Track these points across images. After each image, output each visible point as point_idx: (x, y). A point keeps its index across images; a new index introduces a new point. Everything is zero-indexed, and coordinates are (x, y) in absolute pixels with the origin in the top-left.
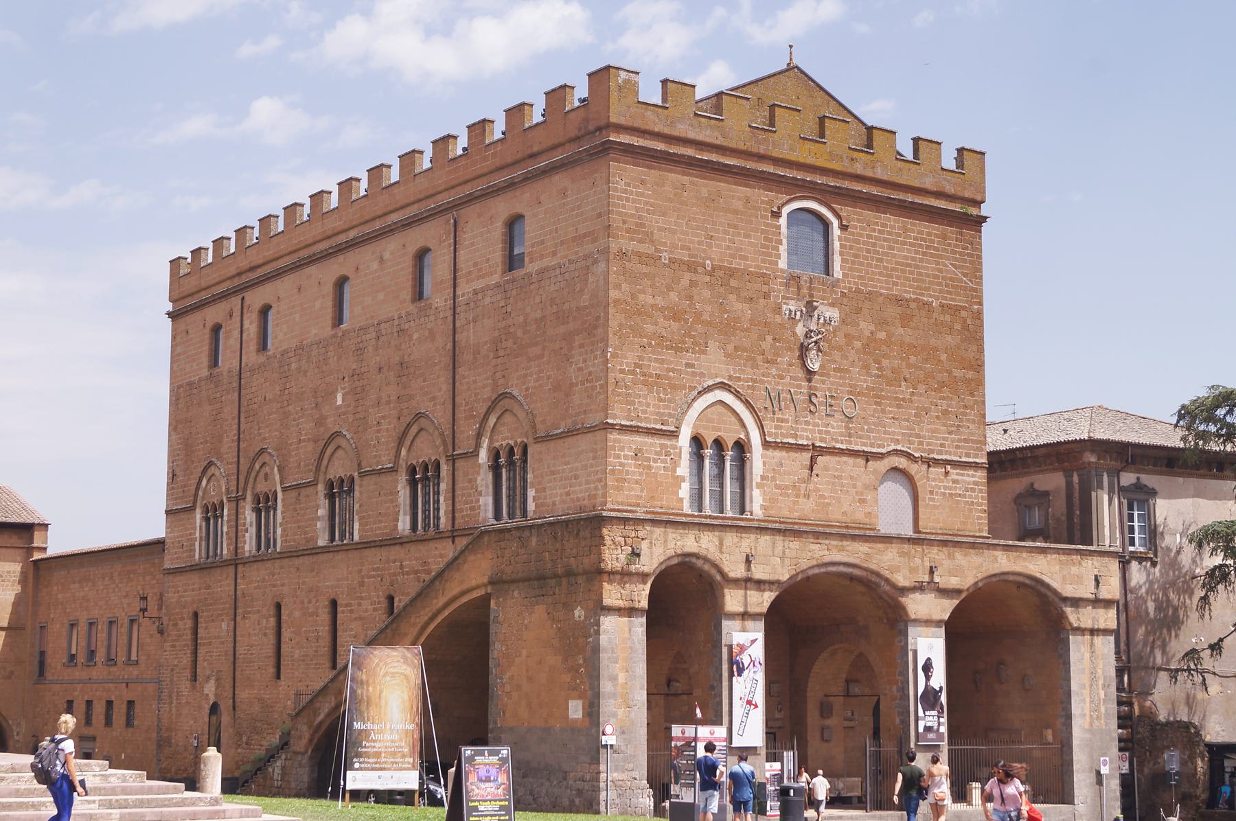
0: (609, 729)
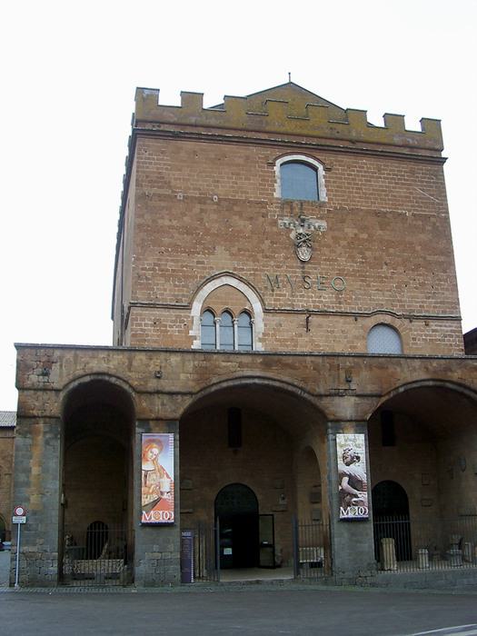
0: (20, 511)
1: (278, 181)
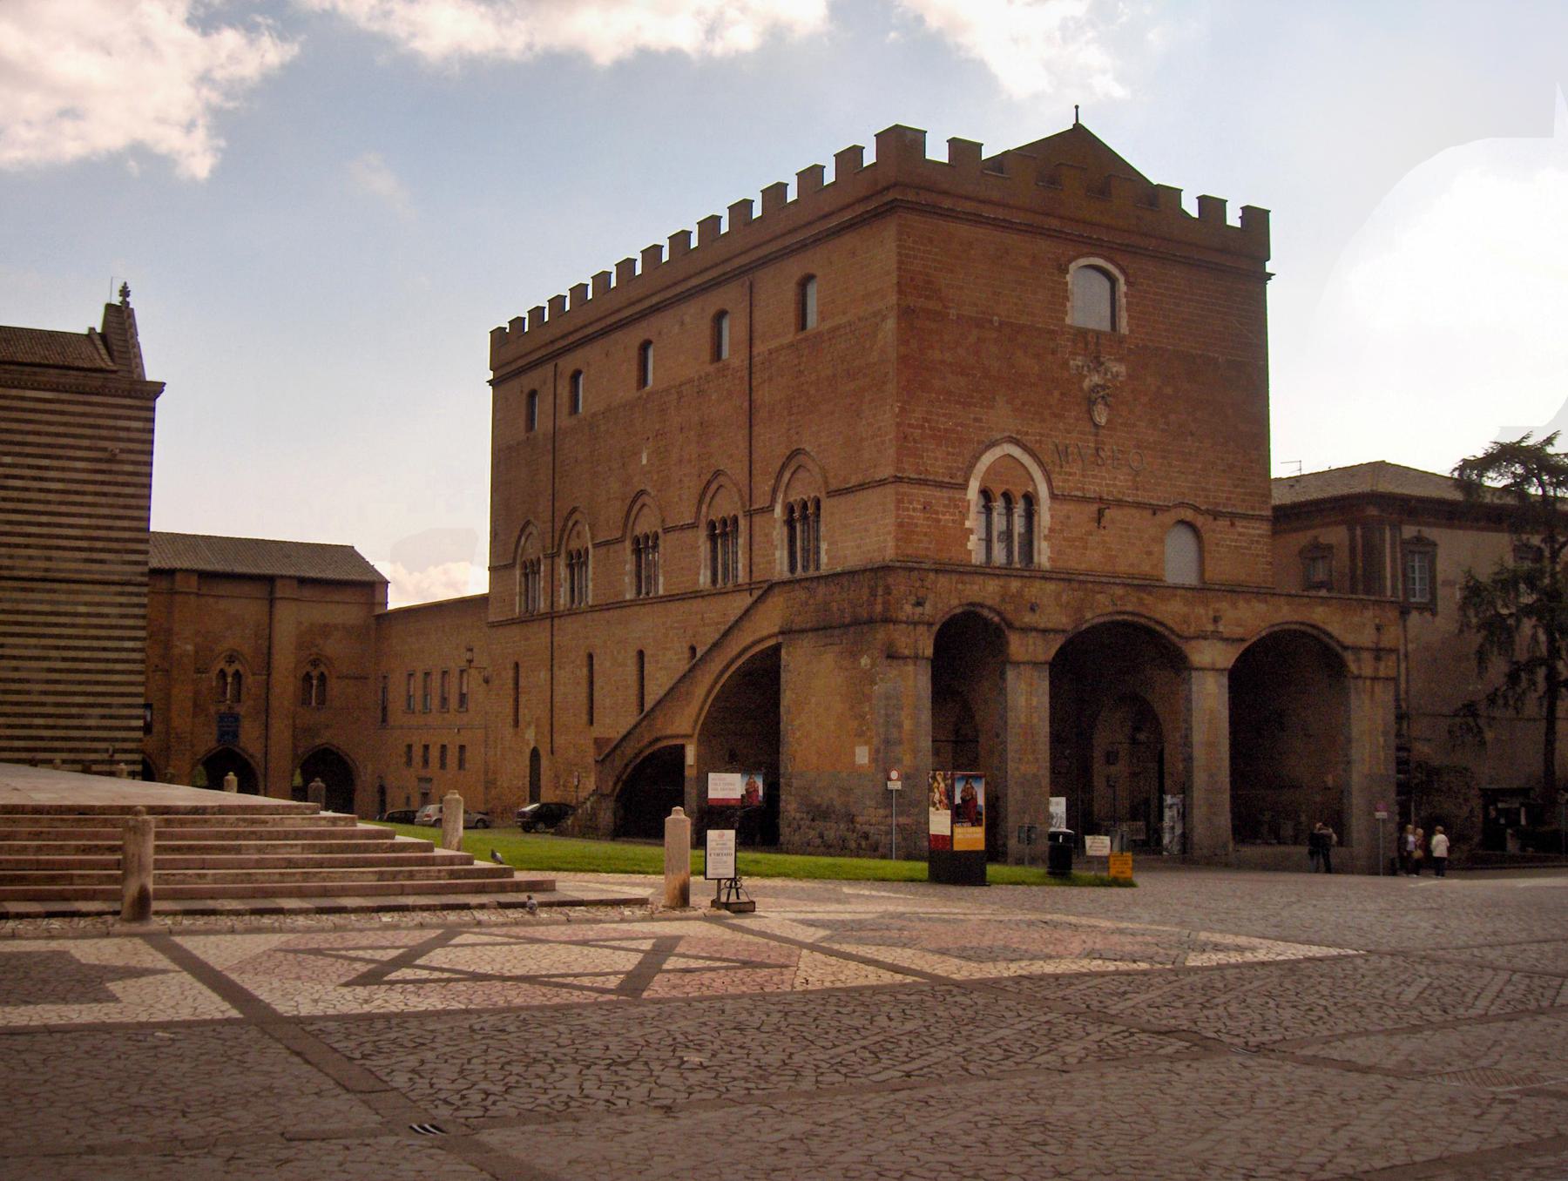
0: (894, 775)
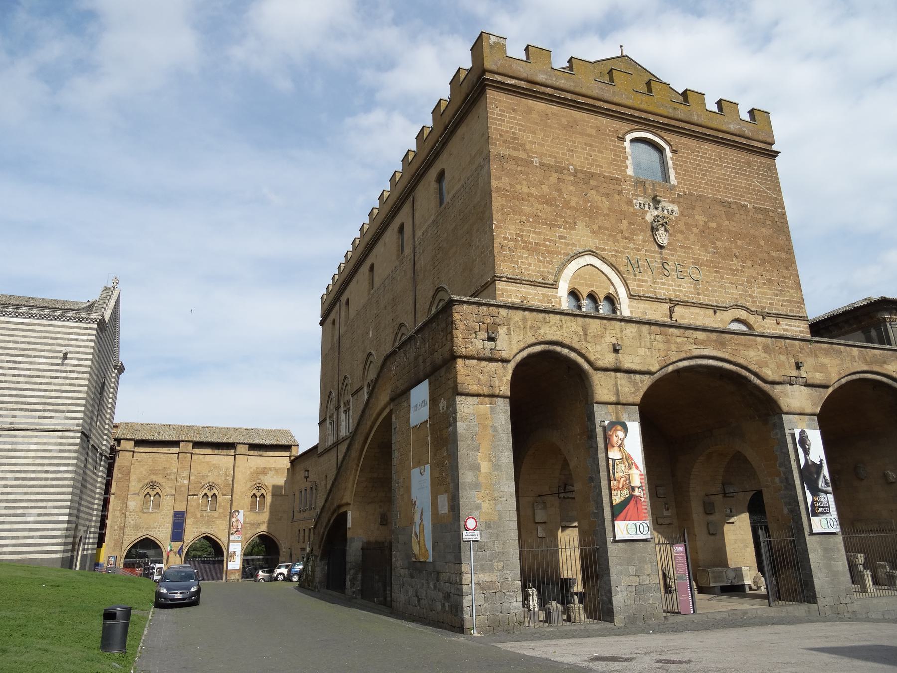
0: (471, 524)
1: (630, 157)
